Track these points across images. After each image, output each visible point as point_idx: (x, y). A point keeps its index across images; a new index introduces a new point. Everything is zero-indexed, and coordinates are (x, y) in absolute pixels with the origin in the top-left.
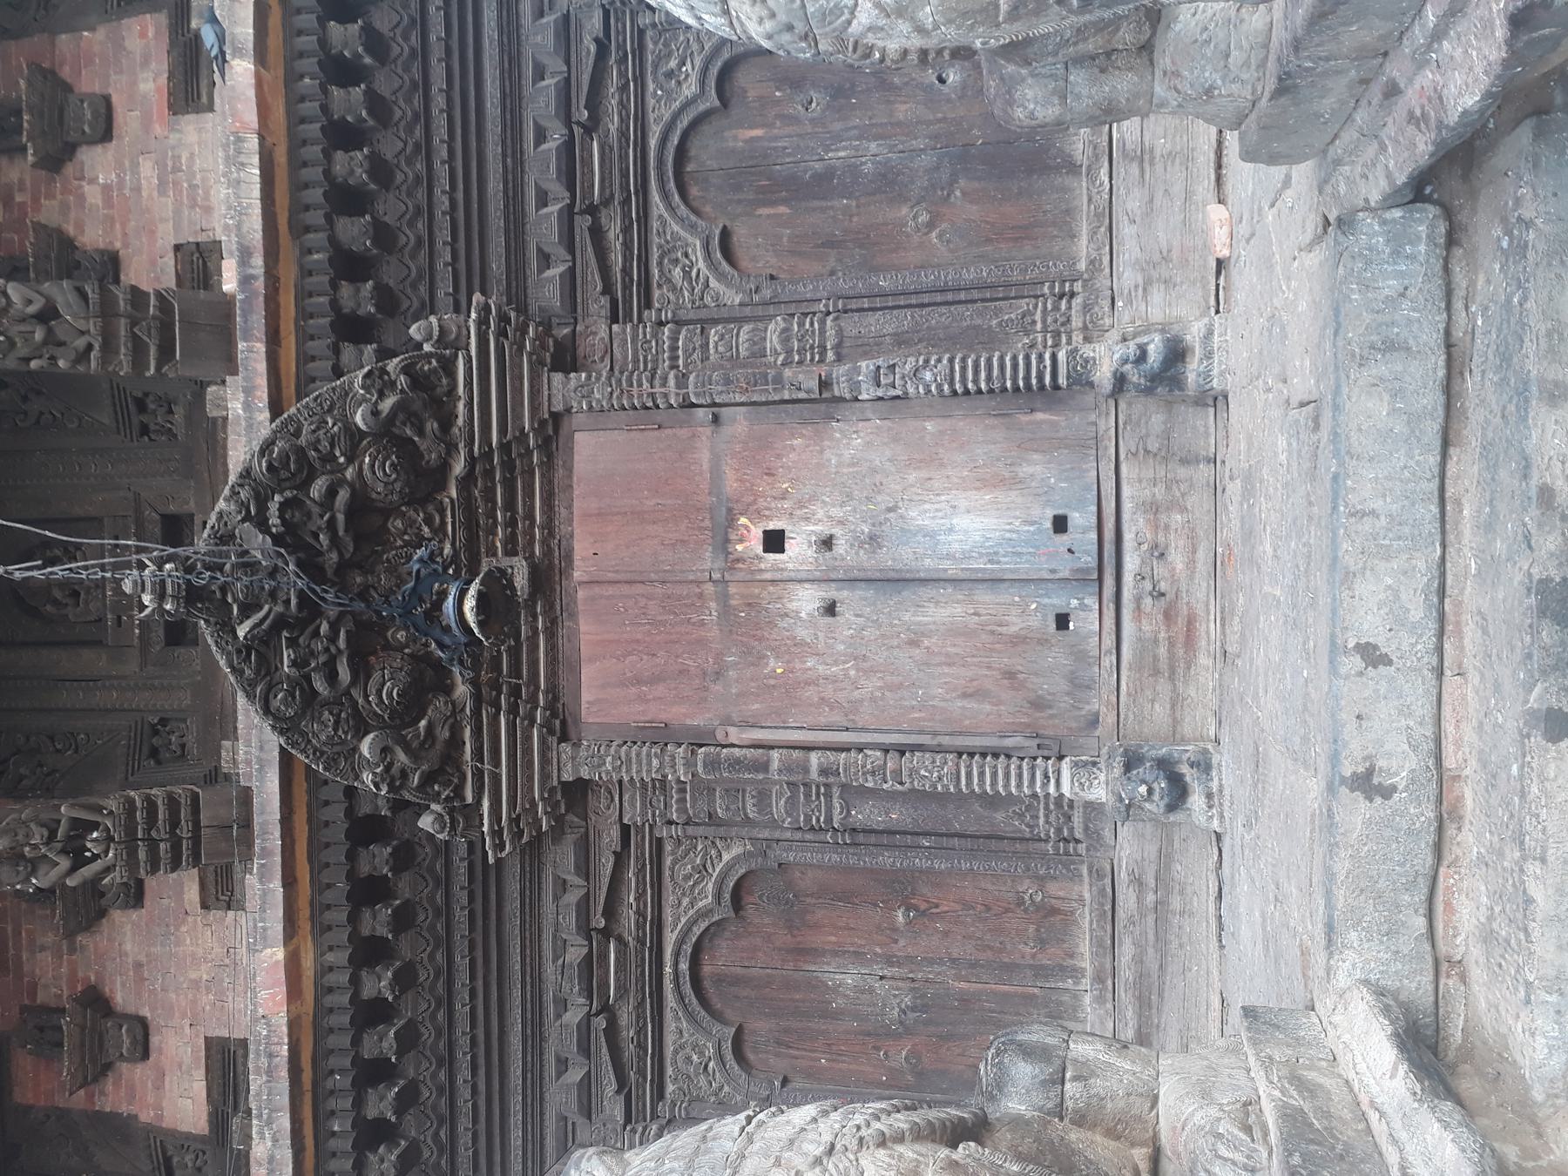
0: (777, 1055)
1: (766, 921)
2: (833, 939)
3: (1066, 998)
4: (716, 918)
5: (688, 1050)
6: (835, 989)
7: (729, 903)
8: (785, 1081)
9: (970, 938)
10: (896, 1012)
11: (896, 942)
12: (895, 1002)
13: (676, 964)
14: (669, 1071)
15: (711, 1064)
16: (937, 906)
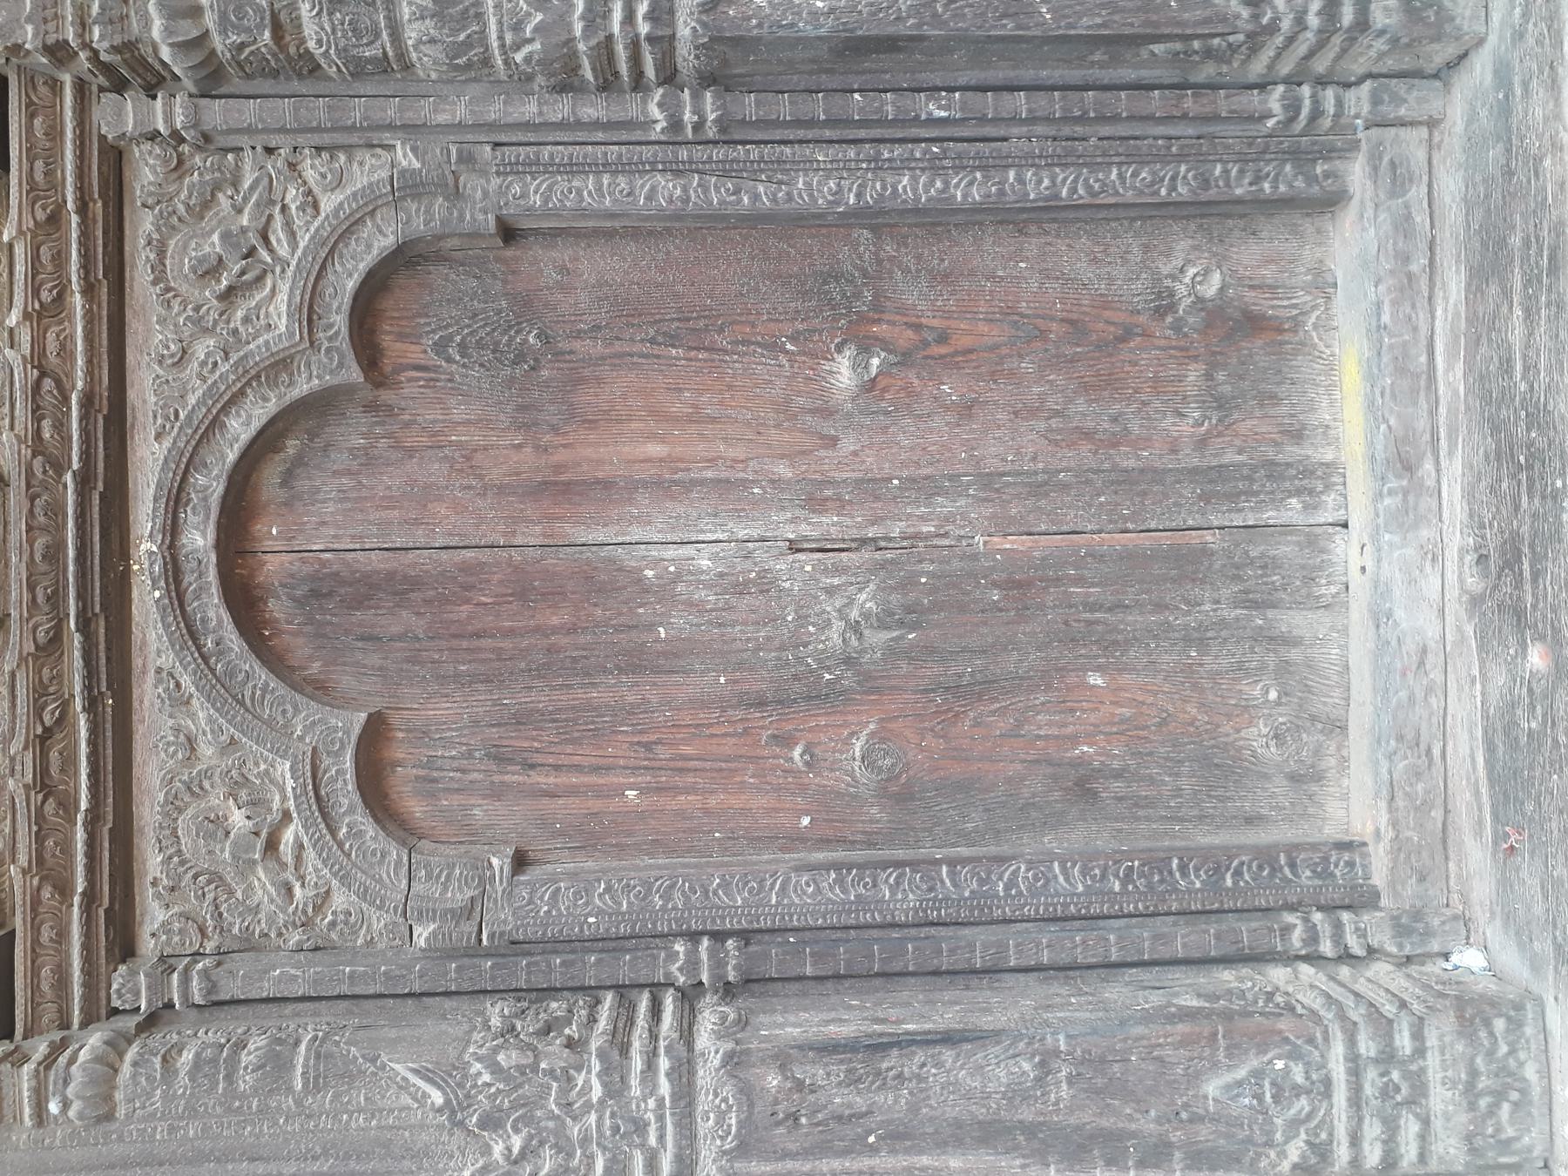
0: (497, 793)
1: (459, 412)
2: (655, 449)
3: (1285, 549)
4: (303, 387)
5: (216, 798)
6: (665, 591)
7: (344, 342)
8: (521, 862)
9: (1033, 412)
10: (834, 635)
11: (833, 442)
12: (830, 607)
13: (172, 530)
14: (152, 862)
15: (288, 836)
16: (943, 338)
